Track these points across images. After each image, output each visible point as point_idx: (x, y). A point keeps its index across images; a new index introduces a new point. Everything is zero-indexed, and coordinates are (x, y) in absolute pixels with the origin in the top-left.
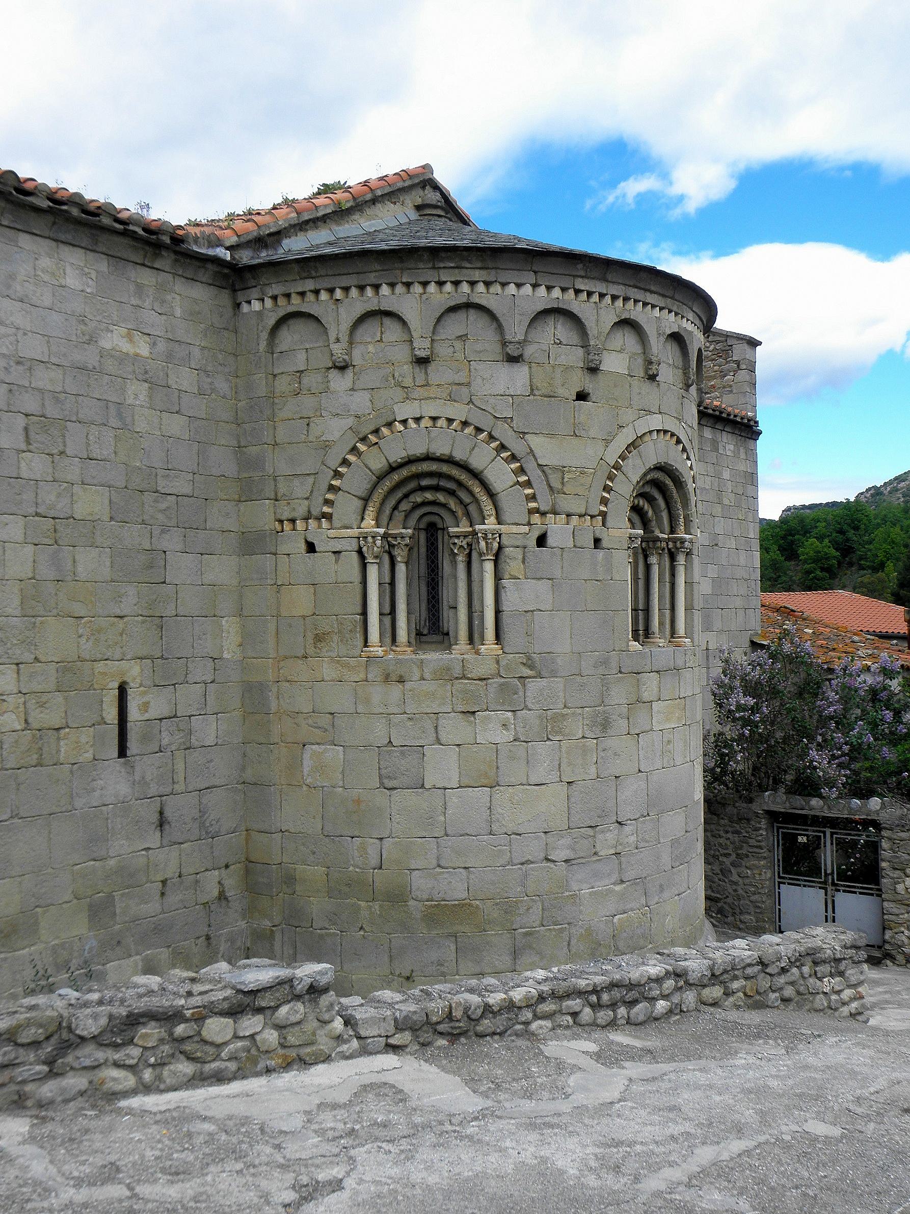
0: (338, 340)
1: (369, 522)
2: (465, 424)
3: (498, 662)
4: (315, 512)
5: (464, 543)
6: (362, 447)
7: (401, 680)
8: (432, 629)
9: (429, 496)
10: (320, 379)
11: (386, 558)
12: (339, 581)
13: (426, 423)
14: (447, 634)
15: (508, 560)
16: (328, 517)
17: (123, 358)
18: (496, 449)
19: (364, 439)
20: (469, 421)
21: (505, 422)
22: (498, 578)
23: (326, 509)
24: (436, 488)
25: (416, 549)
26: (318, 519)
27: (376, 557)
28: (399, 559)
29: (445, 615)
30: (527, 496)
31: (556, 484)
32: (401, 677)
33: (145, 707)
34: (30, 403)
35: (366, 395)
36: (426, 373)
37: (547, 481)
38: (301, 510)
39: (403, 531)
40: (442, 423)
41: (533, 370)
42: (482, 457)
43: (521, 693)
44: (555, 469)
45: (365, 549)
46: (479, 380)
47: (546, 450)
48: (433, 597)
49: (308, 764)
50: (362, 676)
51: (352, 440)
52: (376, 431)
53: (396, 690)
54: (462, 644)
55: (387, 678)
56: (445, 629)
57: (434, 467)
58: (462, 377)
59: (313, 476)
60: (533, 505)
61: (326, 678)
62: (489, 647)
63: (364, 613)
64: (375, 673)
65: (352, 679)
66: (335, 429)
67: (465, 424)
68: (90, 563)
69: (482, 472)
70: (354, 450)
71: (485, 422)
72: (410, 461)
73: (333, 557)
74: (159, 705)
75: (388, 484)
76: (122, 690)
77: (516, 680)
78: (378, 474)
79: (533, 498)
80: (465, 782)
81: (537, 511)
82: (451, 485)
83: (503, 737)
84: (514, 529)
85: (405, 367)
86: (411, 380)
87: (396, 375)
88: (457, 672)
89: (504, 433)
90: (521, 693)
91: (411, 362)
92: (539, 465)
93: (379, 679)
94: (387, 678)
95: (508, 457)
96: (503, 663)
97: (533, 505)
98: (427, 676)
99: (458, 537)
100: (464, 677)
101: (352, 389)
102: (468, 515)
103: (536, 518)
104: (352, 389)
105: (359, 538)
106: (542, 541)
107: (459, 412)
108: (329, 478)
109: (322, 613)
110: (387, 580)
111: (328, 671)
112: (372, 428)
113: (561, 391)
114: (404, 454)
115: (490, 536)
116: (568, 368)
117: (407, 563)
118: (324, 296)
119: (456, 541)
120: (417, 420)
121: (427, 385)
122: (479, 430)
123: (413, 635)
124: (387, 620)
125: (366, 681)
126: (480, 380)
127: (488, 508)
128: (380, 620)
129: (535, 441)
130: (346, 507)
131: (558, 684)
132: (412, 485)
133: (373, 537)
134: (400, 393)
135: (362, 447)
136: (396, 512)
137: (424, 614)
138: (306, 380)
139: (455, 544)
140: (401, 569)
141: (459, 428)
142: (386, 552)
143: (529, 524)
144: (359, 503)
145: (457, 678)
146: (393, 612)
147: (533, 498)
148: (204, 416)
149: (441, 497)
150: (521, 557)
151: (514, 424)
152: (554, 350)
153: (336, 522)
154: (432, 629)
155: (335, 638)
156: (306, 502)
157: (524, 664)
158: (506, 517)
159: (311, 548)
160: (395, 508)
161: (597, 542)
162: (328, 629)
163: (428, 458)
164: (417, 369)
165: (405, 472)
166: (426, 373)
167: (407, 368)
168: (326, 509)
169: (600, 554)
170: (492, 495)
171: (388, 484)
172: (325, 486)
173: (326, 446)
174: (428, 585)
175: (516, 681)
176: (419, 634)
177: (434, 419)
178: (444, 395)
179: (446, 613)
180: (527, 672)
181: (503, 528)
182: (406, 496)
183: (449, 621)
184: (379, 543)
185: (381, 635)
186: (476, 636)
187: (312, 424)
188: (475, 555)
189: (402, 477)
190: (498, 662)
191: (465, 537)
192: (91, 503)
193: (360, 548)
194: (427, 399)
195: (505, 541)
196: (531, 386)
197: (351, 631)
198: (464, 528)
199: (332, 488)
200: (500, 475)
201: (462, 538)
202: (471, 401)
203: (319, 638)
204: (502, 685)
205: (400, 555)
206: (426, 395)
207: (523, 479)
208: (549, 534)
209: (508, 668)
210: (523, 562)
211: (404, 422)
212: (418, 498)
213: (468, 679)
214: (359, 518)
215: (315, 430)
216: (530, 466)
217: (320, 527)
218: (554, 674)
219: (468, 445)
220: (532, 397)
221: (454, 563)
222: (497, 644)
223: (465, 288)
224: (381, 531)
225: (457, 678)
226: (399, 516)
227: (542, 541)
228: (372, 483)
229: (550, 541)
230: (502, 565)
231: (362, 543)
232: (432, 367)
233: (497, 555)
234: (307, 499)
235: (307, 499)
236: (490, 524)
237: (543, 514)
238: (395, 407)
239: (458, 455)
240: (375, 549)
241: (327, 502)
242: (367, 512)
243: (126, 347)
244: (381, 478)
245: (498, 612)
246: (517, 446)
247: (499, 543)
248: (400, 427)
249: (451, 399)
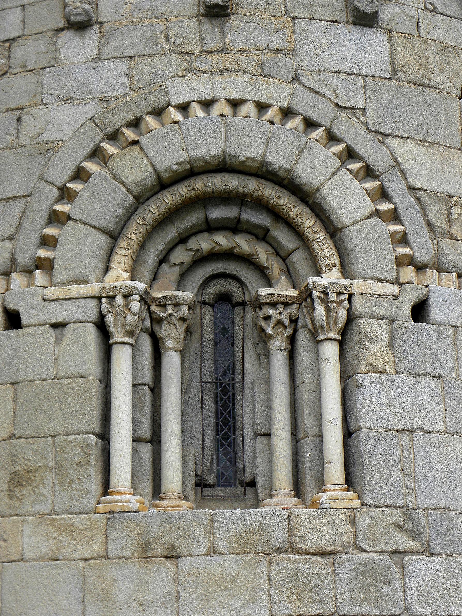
1: (118, 276)
2: (287, 113)
3: (353, 522)
4: (24, 258)
5: (285, 317)
7: (172, 556)
9: (223, 240)
10: (43, 47)
11: (146, 341)
12: (61, 373)
13: (221, 108)
14: (252, 484)
15: (365, 341)
16: (46, 265)
18: (339, 155)
19: (113, 137)
20: (296, 107)
21: (354, 114)
22: (346, 377)
23: (42, 253)
24: (234, 227)
25: (196, 336)
26: (29, 272)
27: (130, 333)
28: (169, 344)
29: (248, 449)
30: (393, 234)
31: (439, 221)
32: (172, 547)
35: (121, 67)
36: (222, 32)
37: (425, 215)
39: (178, 293)
40: (248, 109)
41: (395, 41)
42: (316, 166)
43: (397, 582)
44: (435, 195)
45: (109, 318)
46: (309, 48)
48: (226, 421)
50: (97, 547)
51: (93, 137)
52: (135, 124)
54: (282, 495)
55: (145, 552)
56: (248, 476)
57: (233, 182)
58: (281, 40)
59: (22, 201)
60: (403, 250)
61: (29, 554)
62: (335, 493)
63: (105, 436)
64: (122, 542)
65: (78, 555)
66: (66, 124)
67: (287, 113)
69: (317, 190)
70: (96, 154)
71: (322, 113)
72: (192, 172)
73: (51, 333)
75: (154, 209)
77: (387, 556)
78: (136, 189)
81: (410, 261)
82: (261, 219)
84: (376, 287)
85: (187, 23)
86: (196, 43)
87: (172, 34)
88: (279, 537)
89: (352, 131)
90: (397, 582)
91: (197, 16)
92: (411, 189)
93: (129, 554)
94: (145, 552)
95: (359, 170)
96: (363, 523)
97: (403, 250)
98: (222, 545)
99: (273, 305)
100: (292, 549)
101: (98, 59)
102: (289, 272)
103: (409, 273)
104: (98, 59)
105: (99, 299)
107: (278, 94)
108: (51, 200)
109: (27, 433)
110: (147, 377)
112: (129, 116)
114: (183, 157)
115: (333, 297)
117: (182, 353)
119: (271, 312)
120: (207, 104)
121: (222, 50)
122: (310, 124)
123: (191, 482)
124: (146, 451)
125: (106, 557)
126: (312, 47)
127: (326, 251)
128: (134, 451)
130: (79, 247)
132: (194, 218)
133: (126, 297)
134: (177, 63)
136: (165, 267)
137: (210, 449)
138: (19, 52)
139: (268, 318)
140: (172, 362)
141: (277, 119)
142: (144, 330)
143: (397, 282)
144: (101, 241)
145: (278, 551)
146: (156, 439)
147: (403, 240)
149: (243, 244)
150: (386, 335)
151: (369, 119)
152: (425, 18)
153: (60, 273)
154: (225, 474)
155: (50, 478)
156: (8, 245)
157: (400, 528)
158: (361, 265)
160: (163, 260)
162: (36, 461)
163: (223, 166)
164: (207, 27)
165: (183, 191)
166: (222, 32)
167: (190, 26)
168: (42, 253)
170: (334, 231)
171: (154, 209)
172: (42, 214)
173: (49, 149)
174: (217, 399)
175: (387, 559)
176: (201, 484)
177: (235, 104)
178: (252, 67)
179: (249, 445)
180: (405, 542)
181: (357, 285)
182: (182, 240)
183: (255, 458)
184: (135, 305)
185: (135, 477)
186: (309, 480)
187: (25, 118)
188: (303, 338)
189: (178, 199)
190: (353, 522)
191: (286, 305)
193: (102, 316)
194: (223, 71)
195: (360, 305)
196: (393, 65)
197: (79, 464)
198: (283, 289)
199: (55, 218)
200: (347, 198)
201: (280, 307)
202: (296, 79)
204: (362, 565)
205: (171, 336)
206: (221, 65)
207: (385, 207)
208: (433, 300)
209: (372, 534)
210: (391, 345)
211: (184, 108)
212: (204, 243)
213: (300, 552)
214: (101, 266)
215: (30, 126)
216: (397, 188)
217: (31, 284)
219: (294, 144)
220: (394, 82)
221: (264, 356)
222: (348, 490)
224: (141, 286)
225: (278, 551)
226: (170, 273)
228: (126, 205)
229: (436, 312)
230: (353, 349)
231: (105, 307)
232: (231, 24)
233: (344, 333)
234: (10, 238)
235: (10, 238)
236: (332, 277)
237: (420, 268)
238: (170, 84)
239: (278, 160)
240: (129, 317)
241: (46, 242)
242: (115, 257)
244: (141, 199)
245: (348, 434)
246: (374, 154)
247: (348, 311)
248: (176, 115)
249: (263, 73)
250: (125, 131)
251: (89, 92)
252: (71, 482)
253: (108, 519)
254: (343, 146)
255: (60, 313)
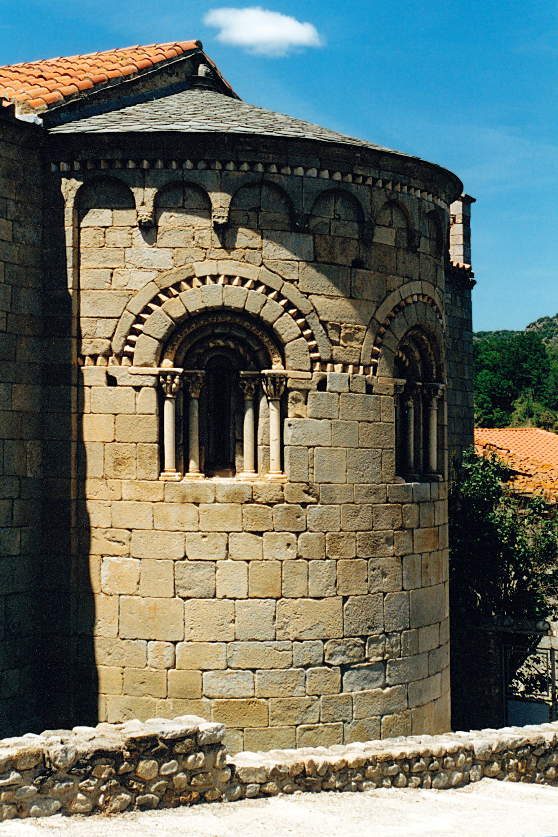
0: (143, 204)
6: (162, 297)
19: (165, 291)
35: (169, 253)
42: (271, 311)
51: (154, 291)
71: (275, 283)
79: (315, 349)
115: (278, 380)
135: (162, 297)
147: (315, 349)
148: (17, 262)
152: (334, 224)
162: (127, 455)
196: (314, 253)
200: (287, 327)
204: (286, 509)
231: (161, 379)
246: (302, 304)
251: (152, 265)
252: (146, 465)
253: (165, 484)
254: (286, 301)
255: (138, 381)
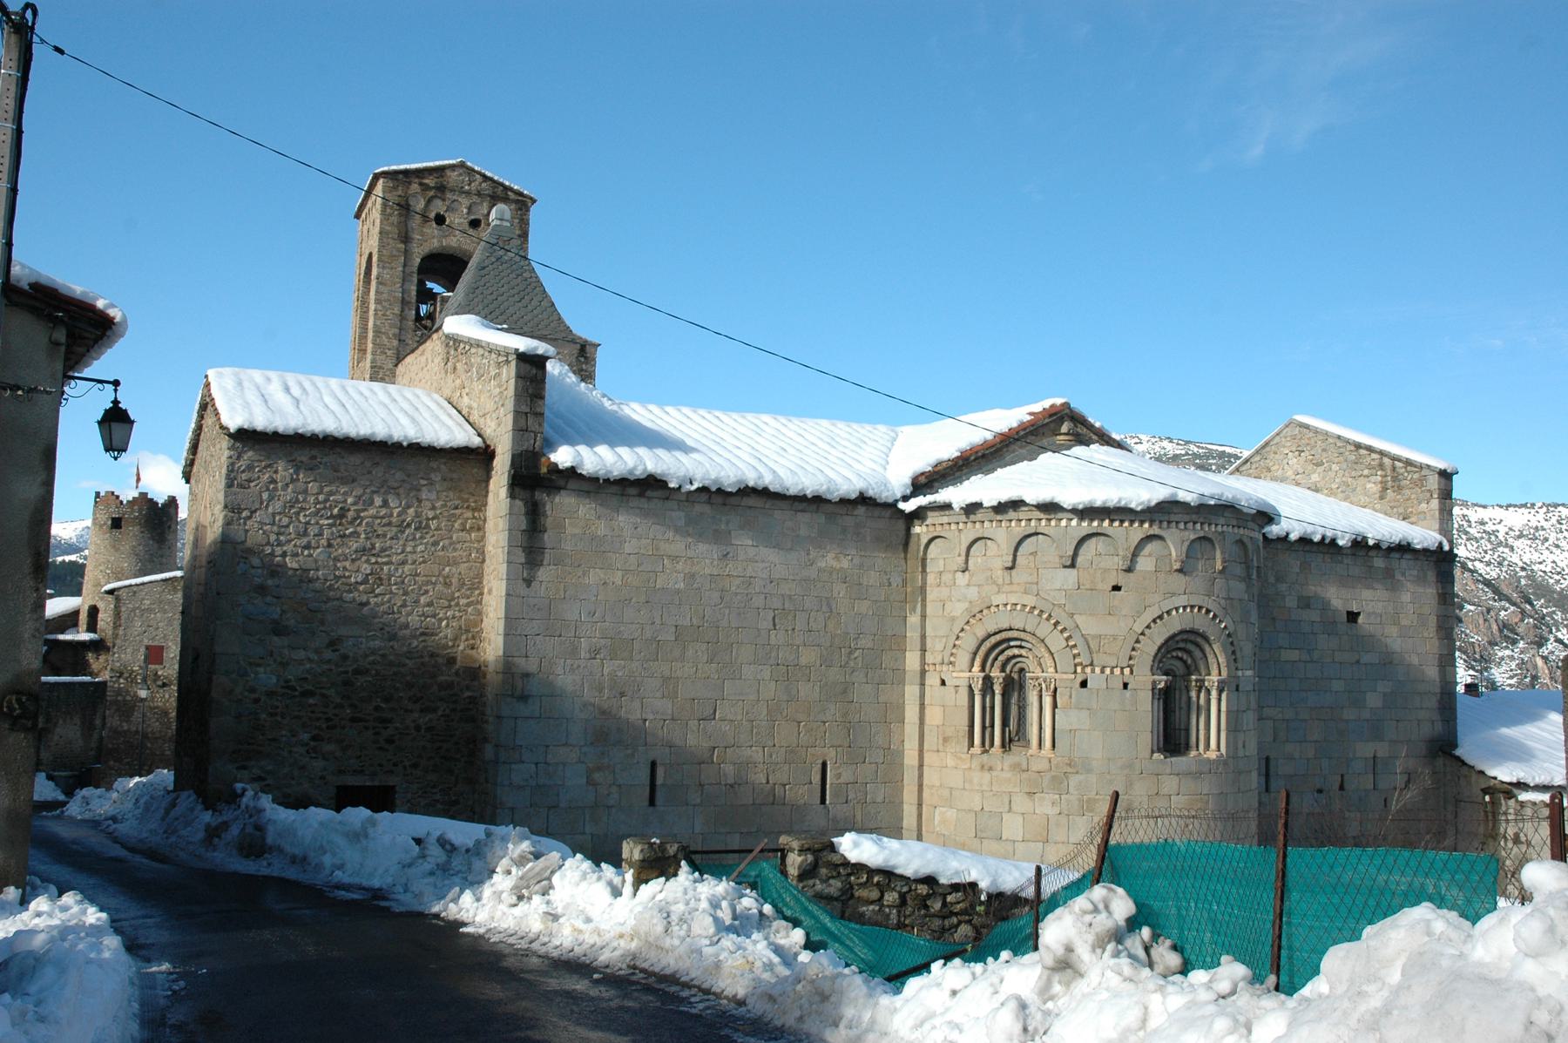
8: (1014, 737)
17: (831, 571)
33: (839, 776)
34: (777, 604)
38: (939, 659)
42: (1044, 629)
44: (1094, 637)
47: (1088, 625)
49: (937, 818)
53: (987, 776)
66: (958, 609)
68: (805, 690)
74: (847, 776)
76: (824, 765)
80: (1028, 837)
83: (1052, 811)
89: (1058, 614)
94: (983, 767)
106: (1084, 684)
107: (1030, 600)
111: (950, 762)
113: (1100, 586)
116: (1106, 571)
118: (953, 527)
129: (1079, 619)
130: (963, 658)
131: (1093, 779)
159: (943, 683)
161: (1125, 686)
169: (1128, 693)
173: (953, 619)
181: (1057, 676)
192: (808, 657)
203: (946, 740)
218: (1089, 771)
223: (1033, 523)
227: (1084, 684)
243: (835, 564)
250: (977, 614)
